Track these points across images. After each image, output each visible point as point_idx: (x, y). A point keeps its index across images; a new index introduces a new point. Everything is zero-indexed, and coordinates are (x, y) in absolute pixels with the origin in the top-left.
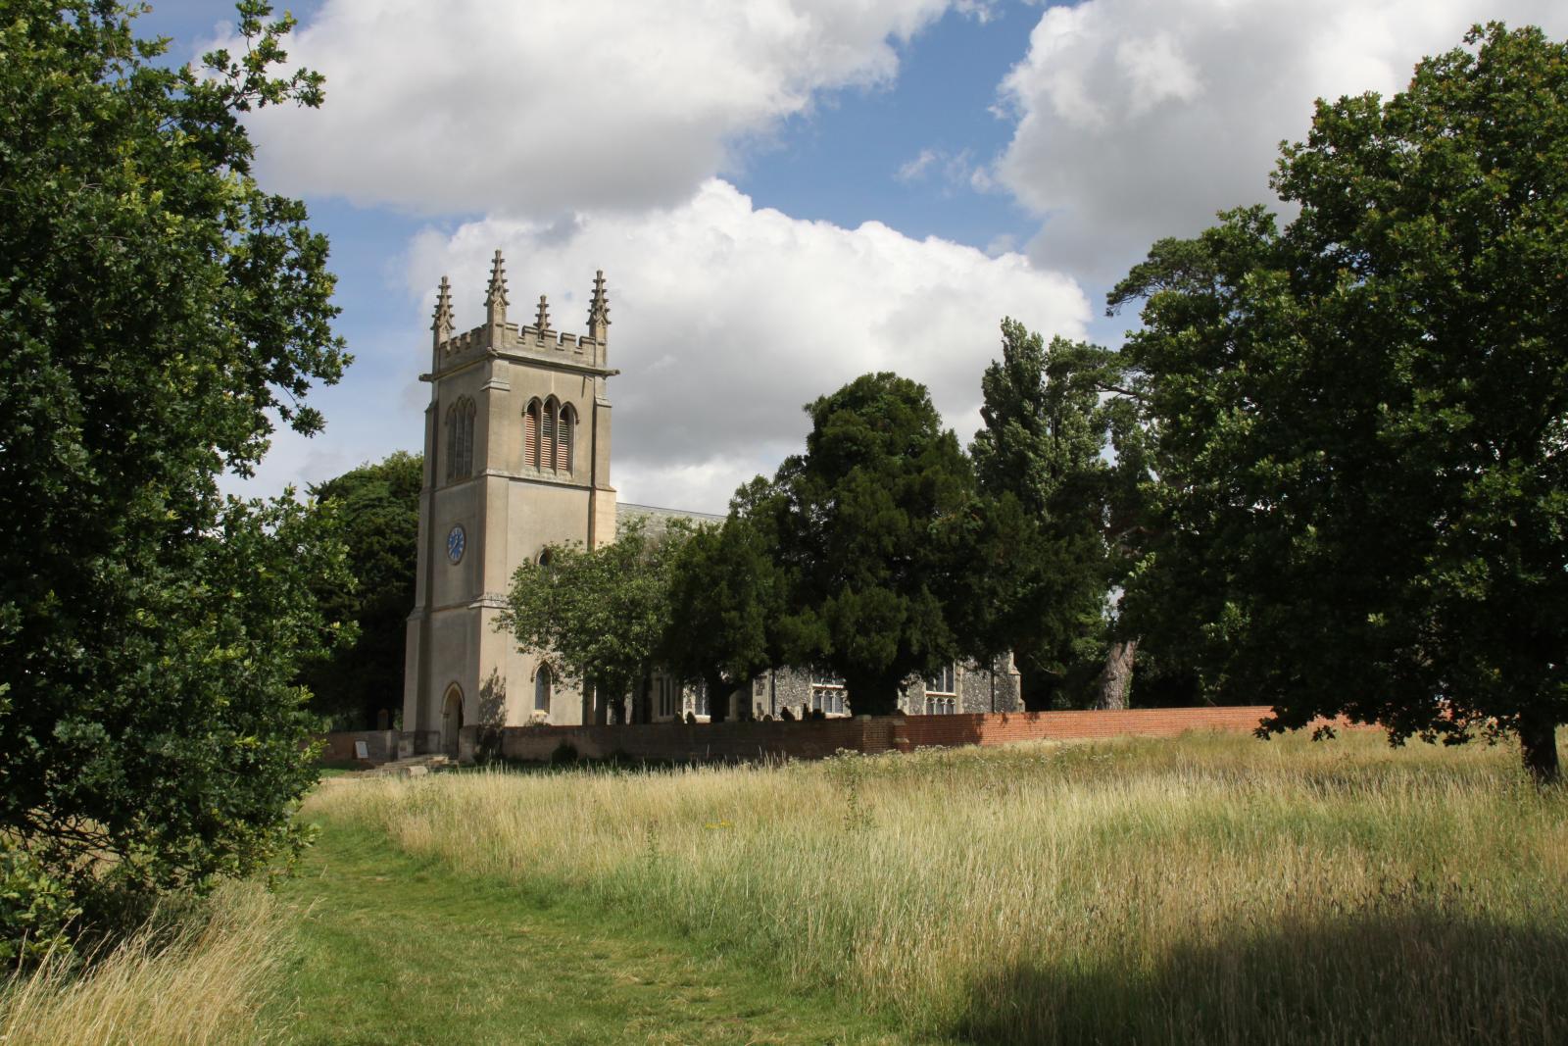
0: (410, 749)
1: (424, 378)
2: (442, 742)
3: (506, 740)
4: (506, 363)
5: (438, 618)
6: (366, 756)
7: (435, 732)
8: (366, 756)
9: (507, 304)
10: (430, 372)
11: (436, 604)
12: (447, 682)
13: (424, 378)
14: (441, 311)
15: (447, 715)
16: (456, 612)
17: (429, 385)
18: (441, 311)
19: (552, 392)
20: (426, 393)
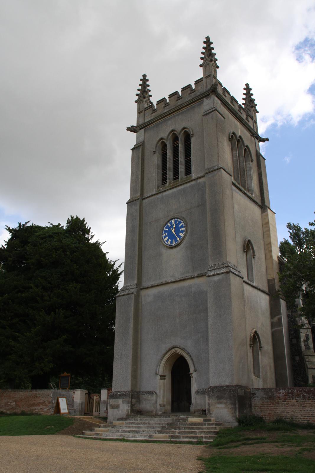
0: (124, 408)
1: (132, 129)
2: (160, 401)
3: (257, 401)
4: (219, 102)
5: (148, 296)
6: (66, 411)
7: (151, 393)
8: (66, 411)
9: (218, 67)
10: (135, 125)
11: (145, 284)
12: (169, 346)
13: (132, 129)
14: (144, 92)
15: (163, 377)
16: (175, 286)
17: (134, 135)
18: (144, 92)
19: (240, 134)
20: (132, 139)
